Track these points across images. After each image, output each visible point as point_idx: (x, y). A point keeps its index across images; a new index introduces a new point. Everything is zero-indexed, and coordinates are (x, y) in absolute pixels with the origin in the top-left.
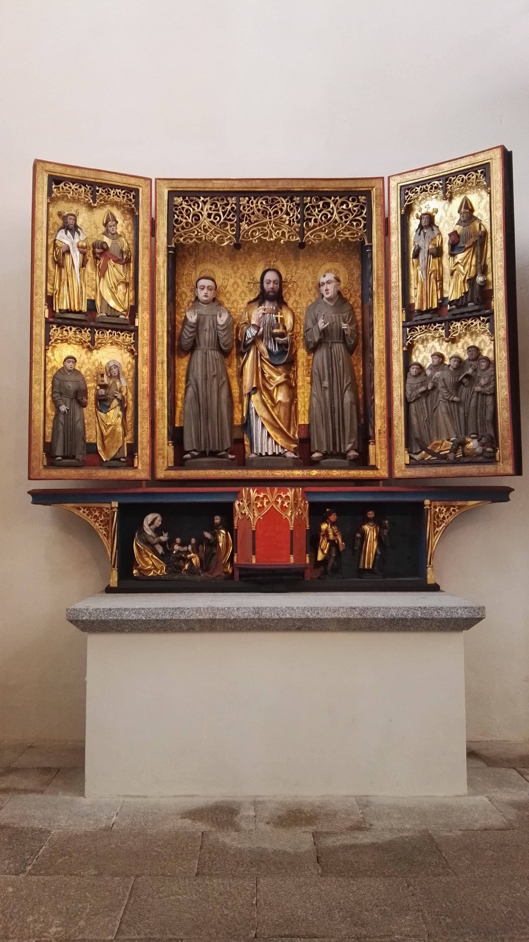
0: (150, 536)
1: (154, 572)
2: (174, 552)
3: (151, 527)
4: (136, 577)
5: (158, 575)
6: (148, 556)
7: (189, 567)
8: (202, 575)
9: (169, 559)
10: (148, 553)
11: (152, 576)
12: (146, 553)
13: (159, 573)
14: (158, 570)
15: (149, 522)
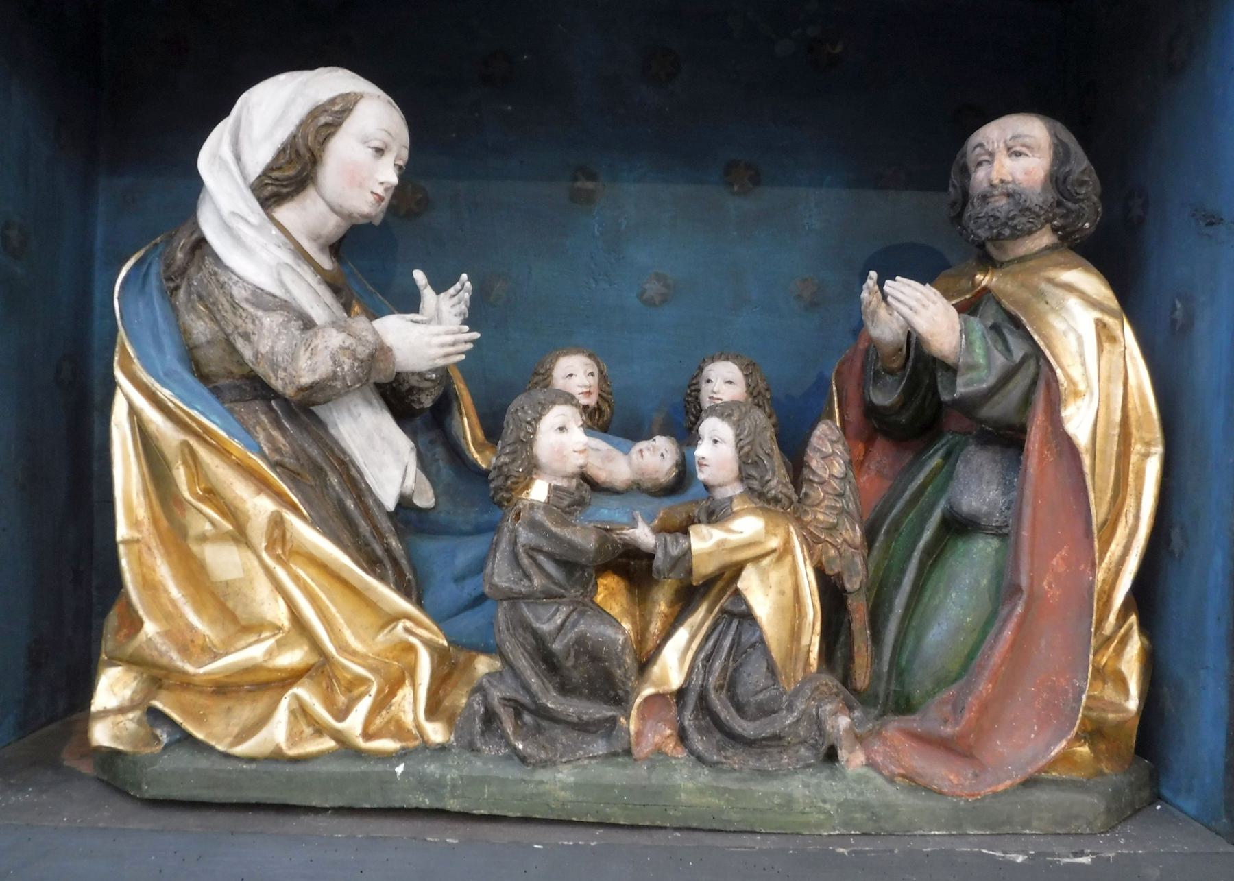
0: (262, 299)
1: (301, 711)
2: (539, 491)
3: (287, 213)
4: (110, 756)
5: (347, 749)
6: (240, 536)
7: (705, 659)
8: (853, 760)
9: (479, 567)
10: (240, 490)
11: (277, 757)
12: (212, 495)
13: (354, 724)
14: (355, 685)
15: (260, 156)
